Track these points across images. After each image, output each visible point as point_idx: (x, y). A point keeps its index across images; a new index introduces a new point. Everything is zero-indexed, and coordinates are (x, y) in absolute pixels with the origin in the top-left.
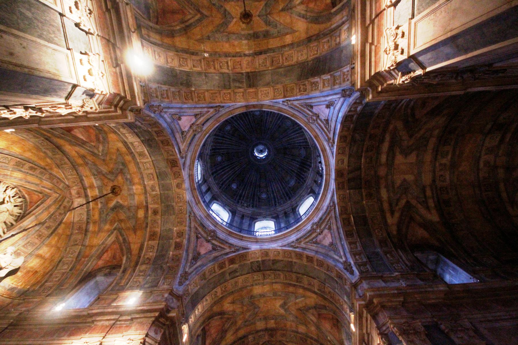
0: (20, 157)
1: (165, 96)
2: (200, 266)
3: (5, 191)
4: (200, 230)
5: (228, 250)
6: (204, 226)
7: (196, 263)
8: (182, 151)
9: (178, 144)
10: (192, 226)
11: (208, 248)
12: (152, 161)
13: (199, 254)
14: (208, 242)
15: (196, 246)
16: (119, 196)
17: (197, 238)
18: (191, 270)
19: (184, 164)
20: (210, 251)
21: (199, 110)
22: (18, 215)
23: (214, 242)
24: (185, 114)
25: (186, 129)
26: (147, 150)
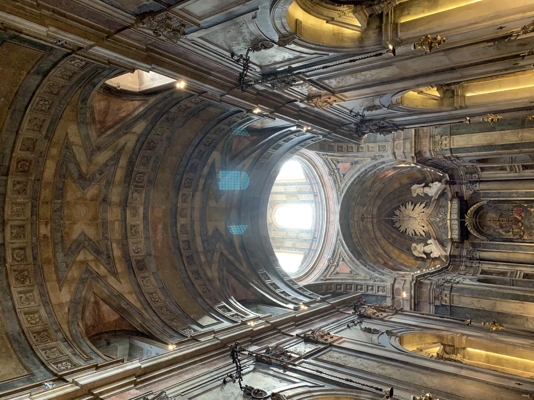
1: (370, 288)
2: (358, 157)
3: (400, 226)
4: (339, 180)
5: (329, 158)
6: (335, 181)
10: (343, 185)
11: (342, 165)
13: (352, 164)
14: (338, 169)
15: (349, 170)
17: (344, 175)
18: (366, 159)
19: (338, 235)
20: (341, 162)
21: (337, 277)
23: (334, 167)
24: (348, 275)
25: (341, 263)
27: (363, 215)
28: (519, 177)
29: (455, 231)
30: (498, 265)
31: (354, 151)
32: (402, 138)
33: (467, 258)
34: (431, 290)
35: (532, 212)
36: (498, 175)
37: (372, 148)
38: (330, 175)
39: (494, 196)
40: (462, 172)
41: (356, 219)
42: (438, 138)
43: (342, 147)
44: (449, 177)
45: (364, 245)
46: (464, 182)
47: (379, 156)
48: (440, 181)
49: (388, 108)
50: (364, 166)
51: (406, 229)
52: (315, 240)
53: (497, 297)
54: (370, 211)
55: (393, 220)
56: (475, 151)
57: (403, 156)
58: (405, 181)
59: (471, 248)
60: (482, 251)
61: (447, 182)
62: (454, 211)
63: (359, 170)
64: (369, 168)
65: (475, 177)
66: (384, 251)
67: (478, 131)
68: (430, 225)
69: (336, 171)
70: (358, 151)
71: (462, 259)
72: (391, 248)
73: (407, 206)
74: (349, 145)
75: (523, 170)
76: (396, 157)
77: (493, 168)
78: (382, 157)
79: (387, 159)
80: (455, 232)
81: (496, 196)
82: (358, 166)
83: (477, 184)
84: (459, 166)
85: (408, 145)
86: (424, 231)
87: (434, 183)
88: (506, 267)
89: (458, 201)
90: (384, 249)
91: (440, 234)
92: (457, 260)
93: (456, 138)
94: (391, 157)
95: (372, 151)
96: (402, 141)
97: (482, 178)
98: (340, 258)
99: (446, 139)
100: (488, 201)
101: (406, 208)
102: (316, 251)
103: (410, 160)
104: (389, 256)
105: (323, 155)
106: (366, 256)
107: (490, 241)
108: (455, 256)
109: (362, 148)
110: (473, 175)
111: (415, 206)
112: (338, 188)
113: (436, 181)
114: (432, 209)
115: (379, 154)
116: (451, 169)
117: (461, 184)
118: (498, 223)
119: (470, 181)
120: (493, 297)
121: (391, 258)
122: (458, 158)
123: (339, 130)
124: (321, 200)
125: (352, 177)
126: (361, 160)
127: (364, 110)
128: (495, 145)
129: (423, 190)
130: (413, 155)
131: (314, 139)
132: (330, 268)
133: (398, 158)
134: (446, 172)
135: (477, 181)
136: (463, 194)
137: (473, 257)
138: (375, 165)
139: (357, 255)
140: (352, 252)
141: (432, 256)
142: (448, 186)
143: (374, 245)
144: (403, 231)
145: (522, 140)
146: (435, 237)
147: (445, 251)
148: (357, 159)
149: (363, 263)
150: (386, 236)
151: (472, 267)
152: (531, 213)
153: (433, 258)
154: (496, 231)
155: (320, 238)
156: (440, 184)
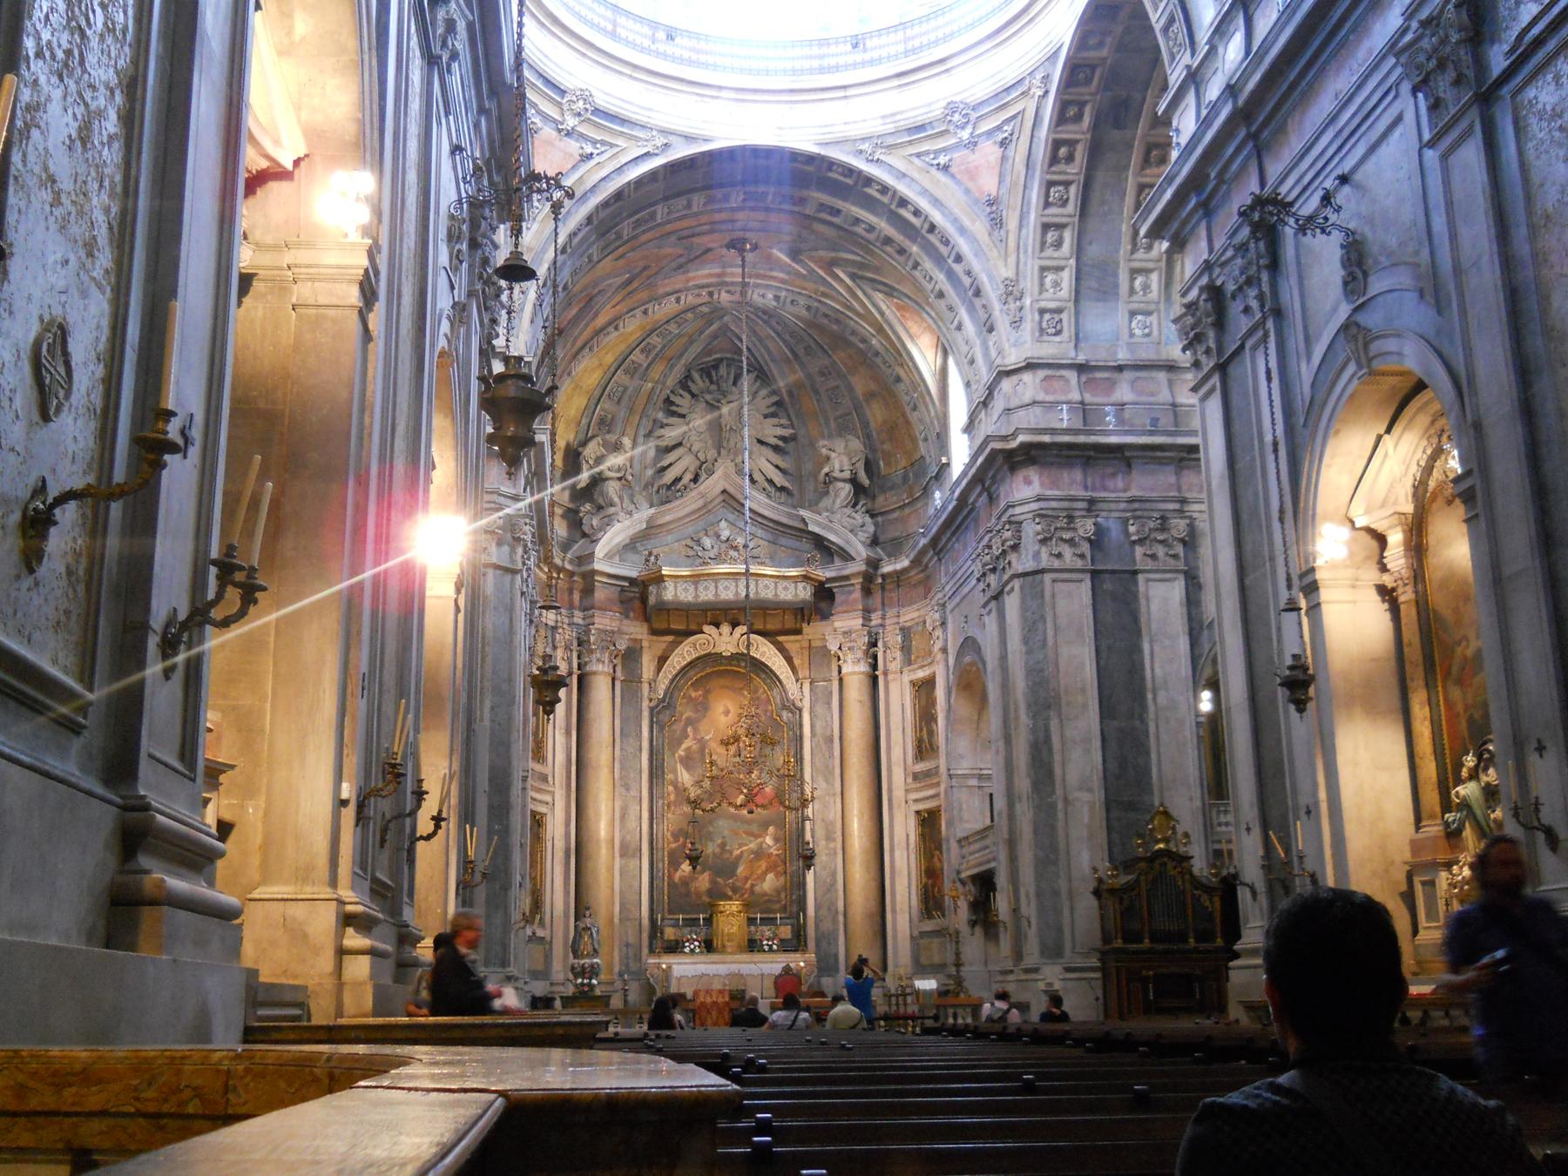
0: (612, 369)
2: (1021, 227)
3: (693, 396)
4: (925, 147)
6: (921, 128)
7: (1007, 232)
8: (645, 150)
9: (620, 170)
12: (666, 199)
14: (975, 144)
16: (762, 243)
17: (945, 168)
18: (1012, 260)
19: (689, 138)
20: (1004, 158)
22: (758, 384)
25: (573, 146)
26: (631, 215)
27: (755, 247)
28: (890, 800)
29: (692, 589)
30: (568, 733)
31: (1047, 212)
32: (1088, 398)
33: (587, 632)
34: (495, 497)
35: (759, 840)
36: (896, 735)
37: (1056, 284)
38: (952, 108)
39: (818, 724)
40: (915, 615)
41: (740, 215)
42: (1086, 527)
43: (1070, 158)
44: (898, 574)
45: (633, 250)
46: (873, 623)
47: (1021, 309)
48: (874, 542)
49: (1349, 329)
50: (979, 253)
51: (683, 416)
52: (661, 35)
53: (493, 721)
54: (764, 277)
55: (716, 367)
56: (1029, 652)
57: (1015, 402)
58: (876, 414)
59: (622, 645)
60: (613, 680)
61: (874, 564)
62: (766, 587)
63: (962, 230)
64: (969, 273)
65: (891, 659)
66: (602, 329)
67: (1102, 662)
68: (700, 503)
69: (965, 134)
70: (1046, 227)
71: (577, 613)
72: (609, 359)
73: (775, 421)
74: (1073, 189)
75: (918, 812)
76: (1009, 373)
77: (926, 716)
78: (1016, 323)
79: (1004, 338)
80: (686, 590)
81: (818, 729)
82: (979, 227)
83: (863, 667)
84: (944, 605)
85: (1064, 418)
86: (678, 480)
87: (868, 519)
88: (560, 757)
89: (804, 601)
90: (611, 329)
91: (669, 538)
92: (576, 596)
93: (1085, 588)
94: (1013, 358)
95: (1042, 284)
96: (1075, 396)
97: (887, 683)
98: (594, 142)
99: (1082, 556)
100: (799, 704)
101: (766, 416)
102: (613, 35)
103: (989, 425)
104: (582, 348)
105: (1046, 79)
106: (595, 259)
107: (652, 709)
108: (588, 591)
109: (1058, 244)
110: (898, 654)
111: (776, 449)
112: (890, 141)
113: (876, 525)
114: (766, 513)
115: (1027, 311)
116: (928, 577)
117: (867, 612)
118: (741, 731)
119: (875, 645)
120: (492, 708)
121: (575, 356)
122: (997, 597)
123: (1242, 133)
124: (836, 68)
125: (936, 202)
126: (1004, 241)
127: (1349, 233)
128: (1048, 719)
129: (844, 481)
130: (1021, 438)
131: (1179, 26)
132: (551, 100)
133: (1006, 385)
134: (916, 562)
135: (874, 666)
136: (825, 616)
137: (591, 652)
138: (978, 293)
139: (602, 215)
140: (618, 195)
141: (588, 506)
142: (863, 568)
143: (630, 288)
144: (672, 403)
145: (1066, 800)
146: (660, 521)
147: (609, 556)
148: (1012, 224)
149: (576, 240)
150: (655, 340)
151: (555, 648)
152: (757, 836)
153: (576, 512)
154: (689, 729)
155: (674, 59)
156: (869, 541)
